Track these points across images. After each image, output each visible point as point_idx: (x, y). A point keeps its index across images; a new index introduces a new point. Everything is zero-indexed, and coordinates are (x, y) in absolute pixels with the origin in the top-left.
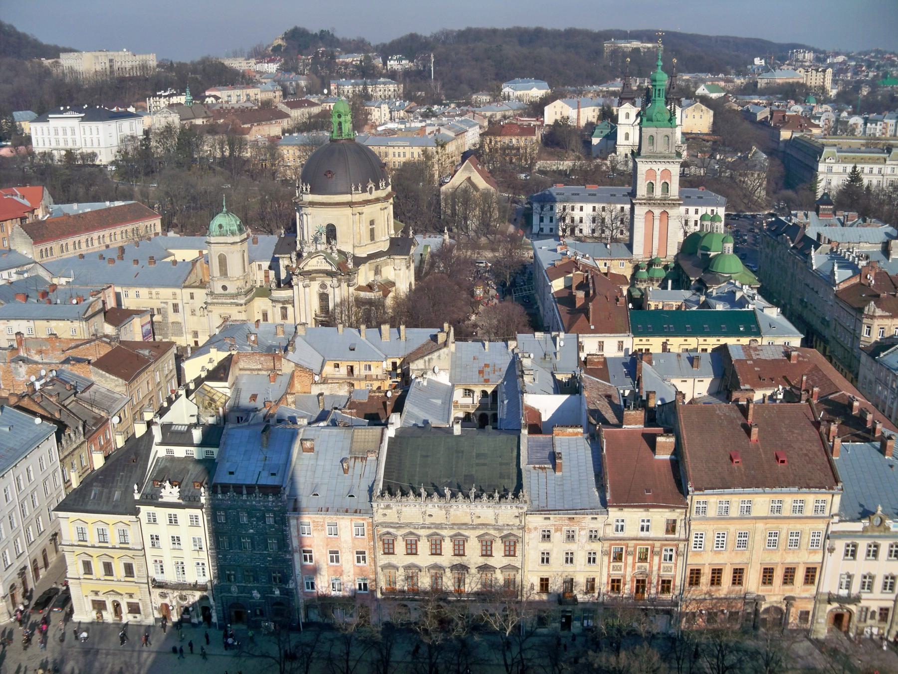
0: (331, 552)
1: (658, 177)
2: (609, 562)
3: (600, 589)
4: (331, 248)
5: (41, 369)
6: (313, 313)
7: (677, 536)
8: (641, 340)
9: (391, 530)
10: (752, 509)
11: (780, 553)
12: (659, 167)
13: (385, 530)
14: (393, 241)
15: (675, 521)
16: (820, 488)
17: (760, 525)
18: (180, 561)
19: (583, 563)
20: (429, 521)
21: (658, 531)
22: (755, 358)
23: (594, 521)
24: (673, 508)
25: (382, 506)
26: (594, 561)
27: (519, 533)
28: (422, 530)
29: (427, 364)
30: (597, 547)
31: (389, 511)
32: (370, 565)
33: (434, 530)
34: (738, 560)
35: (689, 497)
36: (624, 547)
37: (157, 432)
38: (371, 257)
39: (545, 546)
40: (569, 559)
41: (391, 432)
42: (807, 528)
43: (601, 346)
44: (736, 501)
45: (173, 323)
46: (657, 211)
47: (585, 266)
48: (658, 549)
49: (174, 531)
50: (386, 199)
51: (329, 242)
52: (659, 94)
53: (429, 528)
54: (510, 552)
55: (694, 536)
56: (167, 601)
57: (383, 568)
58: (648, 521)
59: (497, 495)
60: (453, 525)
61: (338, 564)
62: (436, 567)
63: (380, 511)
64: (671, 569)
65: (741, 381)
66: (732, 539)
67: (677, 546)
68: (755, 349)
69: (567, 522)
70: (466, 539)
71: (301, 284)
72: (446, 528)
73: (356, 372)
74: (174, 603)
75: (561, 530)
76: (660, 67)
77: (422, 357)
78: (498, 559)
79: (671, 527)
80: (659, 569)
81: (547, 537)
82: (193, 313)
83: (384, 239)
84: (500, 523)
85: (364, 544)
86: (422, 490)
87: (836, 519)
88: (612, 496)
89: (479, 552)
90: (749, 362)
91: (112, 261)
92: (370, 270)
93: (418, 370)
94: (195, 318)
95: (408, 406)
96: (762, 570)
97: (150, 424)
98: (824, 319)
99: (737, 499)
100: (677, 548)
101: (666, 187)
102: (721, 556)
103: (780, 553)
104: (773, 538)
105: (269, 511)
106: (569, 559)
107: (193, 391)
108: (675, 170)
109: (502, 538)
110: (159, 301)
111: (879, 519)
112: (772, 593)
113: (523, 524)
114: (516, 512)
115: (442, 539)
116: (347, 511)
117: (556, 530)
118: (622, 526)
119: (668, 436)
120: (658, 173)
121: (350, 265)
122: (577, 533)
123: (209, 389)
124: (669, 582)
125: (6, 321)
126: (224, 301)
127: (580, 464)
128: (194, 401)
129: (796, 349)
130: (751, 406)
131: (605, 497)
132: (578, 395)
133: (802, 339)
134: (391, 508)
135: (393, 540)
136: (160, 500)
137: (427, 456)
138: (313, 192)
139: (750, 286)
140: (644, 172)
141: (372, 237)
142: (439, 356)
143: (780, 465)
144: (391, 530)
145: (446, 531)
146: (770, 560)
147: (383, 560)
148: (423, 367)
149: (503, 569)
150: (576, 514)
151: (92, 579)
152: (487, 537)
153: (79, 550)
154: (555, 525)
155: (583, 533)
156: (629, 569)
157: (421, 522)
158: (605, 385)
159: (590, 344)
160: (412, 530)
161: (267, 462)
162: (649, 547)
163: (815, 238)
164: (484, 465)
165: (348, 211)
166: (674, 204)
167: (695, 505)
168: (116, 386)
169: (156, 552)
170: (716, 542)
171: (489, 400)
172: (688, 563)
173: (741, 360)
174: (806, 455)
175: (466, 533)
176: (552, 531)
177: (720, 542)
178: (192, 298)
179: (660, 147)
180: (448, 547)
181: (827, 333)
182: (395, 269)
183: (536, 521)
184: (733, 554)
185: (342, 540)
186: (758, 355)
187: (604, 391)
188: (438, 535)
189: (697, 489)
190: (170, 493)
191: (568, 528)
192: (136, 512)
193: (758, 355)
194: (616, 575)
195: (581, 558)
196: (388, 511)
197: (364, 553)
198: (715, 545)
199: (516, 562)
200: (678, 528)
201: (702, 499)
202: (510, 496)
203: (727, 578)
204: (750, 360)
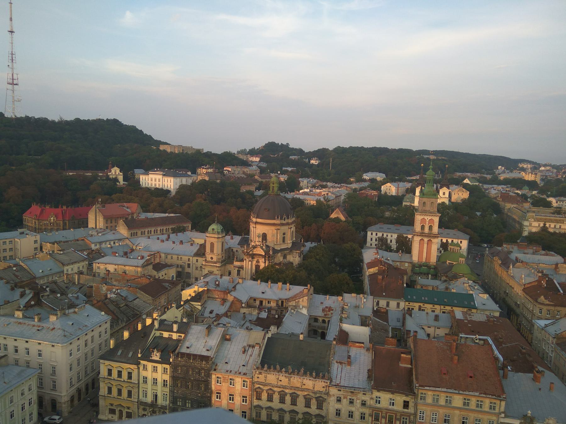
0: (230, 395)
1: (427, 223)
2: (372, 421)
4: (263, 244)
5: (114, 288)
6: (252, 274)
7: (409, 411)
8: (409, 303)
9: (261, 386)
10: (452, 402)
12: (428, 218)
13: (259, 386)
14: (293, 243)
15: (408, 402)
16: (492, 395)
17: (457, 412)
18: (155, 392)
19: (358, 419)
20: (280, 383)
21: (399, 407)
23: (364, 396)
24: (407, 395)
25: (257, 373)
26: (364, 419)
27: (325, 397)
33: (282, 389)
37: (156, 324)
38: (282, 250)
39: (338, 406)
41: (269, 335)
43: (388, 304)
44: (443, 396)
45: (187, 273)
46: (426, 240)
47: (385, 263)
48: (399, 417)
50: (292, 223)
51: (262, 242)
52: (430, 182)
53: (279, 387)
54: (320, 407)
58: (393, 400)
59: (314, 374)
60: (291, 388)
61: (233, 402)
62: (281, 410)
67: (409, 416)
69: (350, 394)
70: (298, 396)
71: (247, 260)
72: (288, 389)
73: (264, 304)
75: (347, 399)
76: (431, 169)
78: (313, 409)
79: (406, 405)
81: (339, 400)
82: (197, 268)
83: (289, 242)
84: (316, 390)
85: (247, 392)
89: (304, 404)
90: (465, 321)
91: (163, 241)
92: (281, 256)
93: (292, 306)
94: (197, 271)
97: (154, 320)
98: (516, 303)
99: (444, 395)
100: (409, 419)
101: (431, 228)
105: (203, 369)
107: (182, 305)
108: (436, 220)
110: (182, 262)
111: (530, 419)
113: (327, 391)
115: (286, 394)
116: (240, 373)
117: (344, 398)
120: (428, 220)
121: (271, 253)
122: (355, 401)
123: (191, 305)
125: (105, 264)
126: (211, 264)
127: (361, 363)
128: (182, 311)
133: (500, 313)
136: (150, 358)
138: (257, 218)
139: (474, 281)
140: (420, 220)
141: (284, 241)
142: (303, 300)
144: (261, 386)
148: (295, 305)
150: (355, 390)
151: (111, 397)
155: (358, 401)
157: (276, 383)
159: (383, 303)
161: (206, 344)
163: (514, 259)
165: (273, 228)
166: (435, 236)
167: (420, 395)
168: (148, 300)
169: (144, 385)
174: (486, 375)
175: (299, 393)
176: (342, 398)
178: (197, 261)
179: (428, 208)
180: (288, 399)
181: (518, 311)
182: (293, 257)
183: (333, 391)
185: (236, 389)
186: (471, 318)
188: (284, 392)
189: (420, 386)
190: (156, 356)
191: (350, 397)
192: (138, 364)
193: (471, 318)
196: (260, 376)
197: (246, 397)
198: (431, 420)
199: (323, 413)
201: (424, 392)
204: (465, 320)
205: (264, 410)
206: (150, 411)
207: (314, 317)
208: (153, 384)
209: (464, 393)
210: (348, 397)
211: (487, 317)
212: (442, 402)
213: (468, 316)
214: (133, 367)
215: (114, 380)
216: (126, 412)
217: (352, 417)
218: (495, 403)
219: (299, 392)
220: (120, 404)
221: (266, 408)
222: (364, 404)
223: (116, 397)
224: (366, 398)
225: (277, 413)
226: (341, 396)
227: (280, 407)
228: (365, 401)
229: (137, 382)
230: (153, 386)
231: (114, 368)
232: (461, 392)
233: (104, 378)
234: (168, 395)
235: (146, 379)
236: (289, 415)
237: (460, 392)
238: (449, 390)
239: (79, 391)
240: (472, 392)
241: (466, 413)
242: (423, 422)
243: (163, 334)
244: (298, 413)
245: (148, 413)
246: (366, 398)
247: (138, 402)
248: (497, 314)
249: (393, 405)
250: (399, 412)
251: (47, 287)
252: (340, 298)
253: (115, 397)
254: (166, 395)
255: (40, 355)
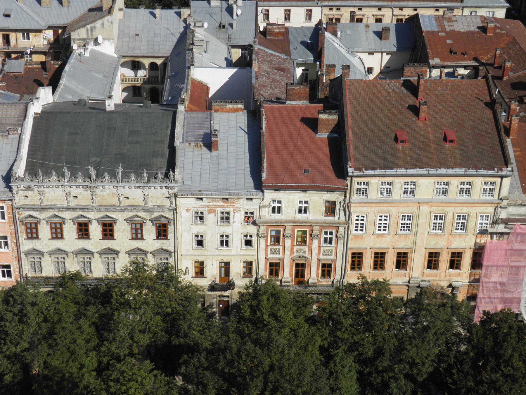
2: (267, 246)
3: (257, 274)
7: (337, 217)
9: (34, 213)
11: (446, 237)
13: (27, 213)
15: (334, 203)
17: (425, 209)
20: (73, 203)
22: (448, 29)
23: (249, 202)
25: (22, 188)
27: (170, 216)
28: (67, 213)
29: (90, 33)
30: (252, 230)
31: (30, 192)
32: (13, 251)
34: (403, 245)
35: (349, 179)
36: (282, 230)
39: (199, 229)
40: (225, 242)
42: (475, 212)
43: (287, 17)
44: (399, 183)
48: (318, 232)
53: (74, 210)
55: (355, 218)
57: (27, 254)
58: (306, 202)
63: (21, 192)
64: (331, 252)
65: (430, 54)
66: (395, 222)
68: (450, 20)
69: (221, 203)
72: (92, 210)
75: (214, 211)
77: (84, 26)
79: (331, 209)
80: (319, 253)
84: (150, 204)
86: (65, 170)
87: (505, 203)
88: (268, 175)
93: (80, 39)
95: (64, 81)
96: (427, 255)
100: (337, 232)
102: (384, 239)
103: (446, 237)
104: (438, 221)
106: (225, 242)
109: (152, 221)
112: (437, 279)
114: (165, 192)
117: (210, 212)
118: (279, 208)
119: (330, 114)
122: (231, 214)
124: (330, 266)
129: (497, 20)
130: (422, 81)
131: (261, 177)
132: (249, 68)
134: (33, 190)
135: (36, 224)
137: (76, 134)
143: (447, 145)
144: (34, 213)
145: (93, 213)
146: (435, 244)
147: (26, 245)
148: (85, 36)
149: (154, 253)
152: (137, 219)
154: (208, 206)
156: (287, 253)
157: (65, 204)
158: (280, 58)
160: (57, 213)
162: (308, 230)
164: (137, 142)
170: (378, 225)
171: (159, 73)
172: (349, 246)
173: (433, 32)
176: (206, 213)
177: (383, 225)
180: (95, 230)
184: (396, 237)
187: (278, 64)
191: (222, 209)
194: (274, 257)
195: (237, 241)
196: (29, 193)
198: (377, 228)
199: (168, 245)
200: (337, 211)
202: (160, 176)
203: (390, 261)
204: (440, 32)
205: (47, 256)
207: (132, 59)
209: (438, 172)
210: (217, 209)
211: (482, 22)
212: (397, 194)
213: (445, 23)
217: (227, 245)
218: (493, 184)
219: (116, 213)
221: (51, 253)
222: (249, 218)
224: (253, 206)
225: (76, 259)
226: (201, 210)
227: (80, 247)
228: (252, 213)
232: (432, 171)
236: (100, 259)
237: (430, 172)
238: (410, 171)
240: (452, 169)
241: (440, 208)
242: (362, 235)
244: (119, 252)
246: (253, 206)
248: (501, 14)
249: (306, 212)
250: (317, 223)
252: (185, 12)
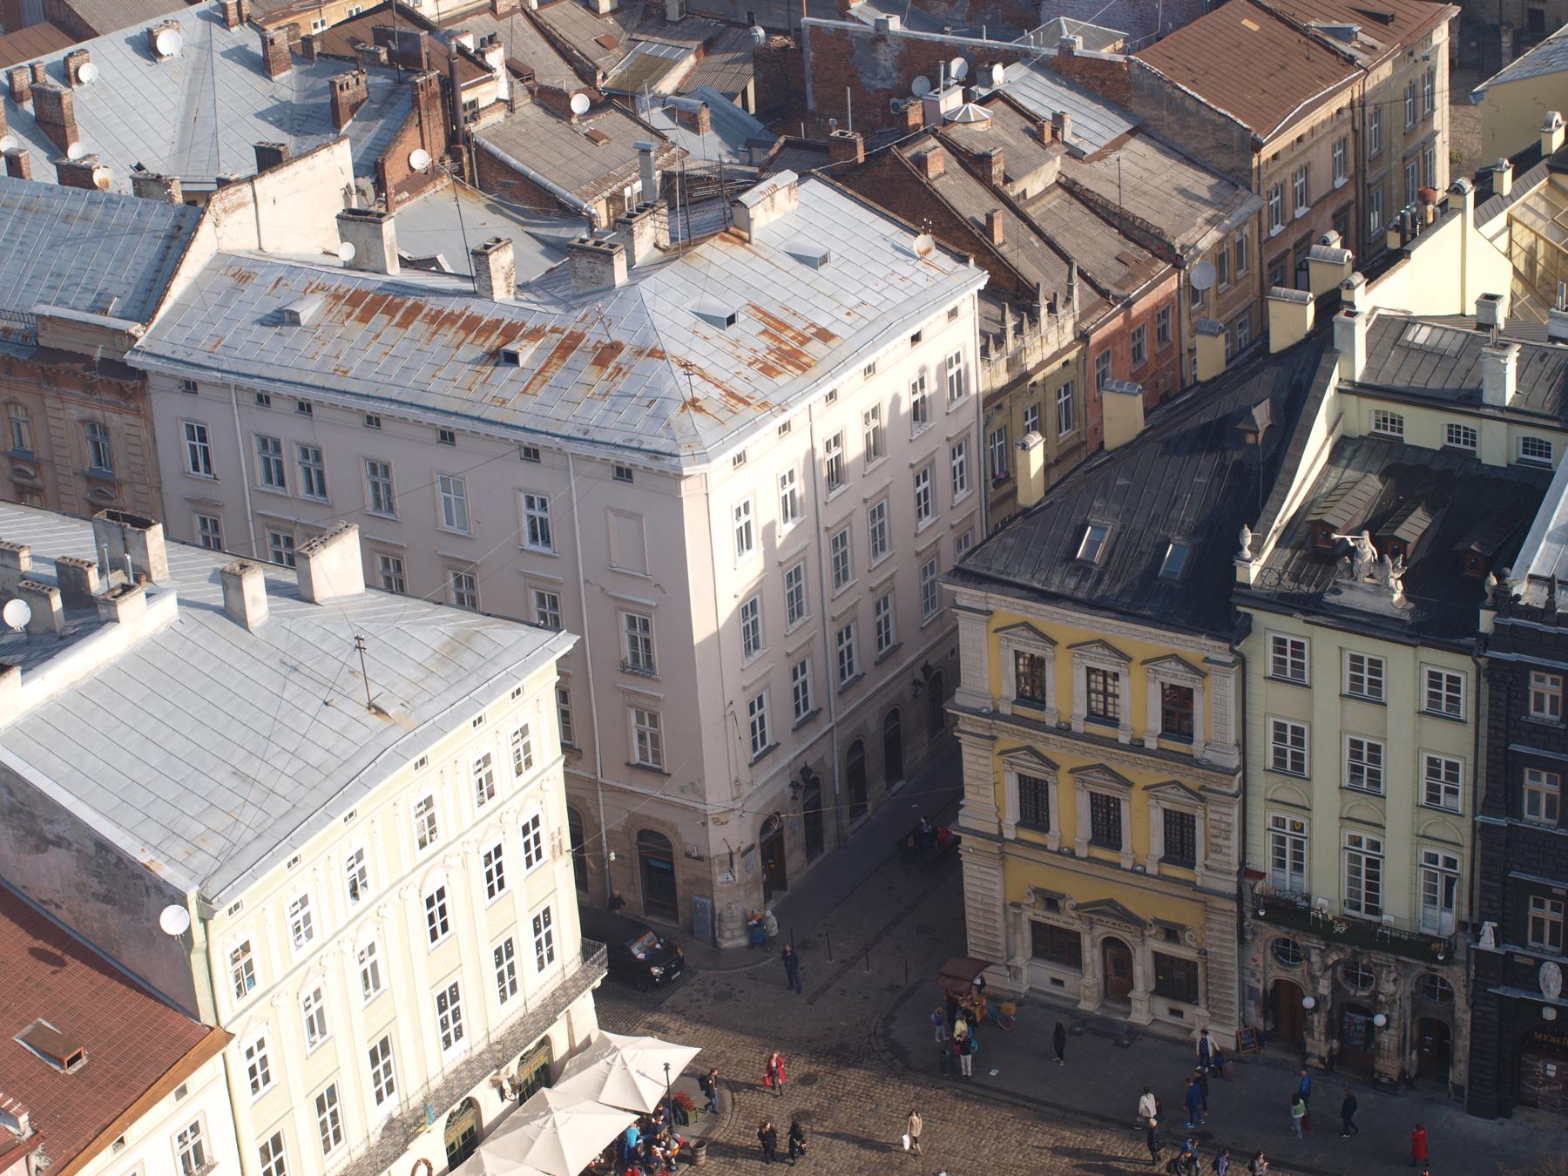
49: (1362, 721)
56: (1296, 974)
74: (1324, 988)
153: (1009, 739)
169: (1288, 790)
206: (1326, 968)
208: (1346, 782)
214: (1196, 647)
215: (1064, 730)
216: (1157, 956)
220: (1111, 903)
223: (1082, 852)
229: (1234, 761)
230: (1352, 797)
231: (1060, 649)
233: (995, 714)
234: (1463, 868)
235: (1298, 742)
239: (807, 782)
243: (1397, 422)
245: (1314, 979)
247: (1239, 898)
251: (490, 41)
253: (1072, 854)
254: (1450, 863)
255: (540, 532)
